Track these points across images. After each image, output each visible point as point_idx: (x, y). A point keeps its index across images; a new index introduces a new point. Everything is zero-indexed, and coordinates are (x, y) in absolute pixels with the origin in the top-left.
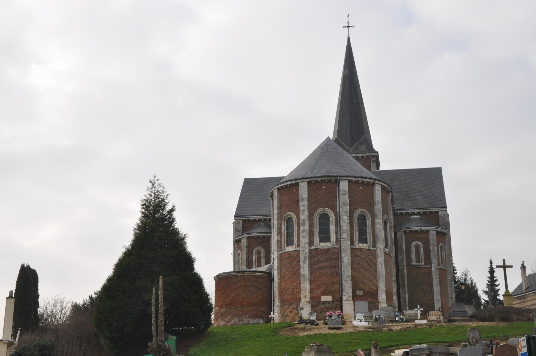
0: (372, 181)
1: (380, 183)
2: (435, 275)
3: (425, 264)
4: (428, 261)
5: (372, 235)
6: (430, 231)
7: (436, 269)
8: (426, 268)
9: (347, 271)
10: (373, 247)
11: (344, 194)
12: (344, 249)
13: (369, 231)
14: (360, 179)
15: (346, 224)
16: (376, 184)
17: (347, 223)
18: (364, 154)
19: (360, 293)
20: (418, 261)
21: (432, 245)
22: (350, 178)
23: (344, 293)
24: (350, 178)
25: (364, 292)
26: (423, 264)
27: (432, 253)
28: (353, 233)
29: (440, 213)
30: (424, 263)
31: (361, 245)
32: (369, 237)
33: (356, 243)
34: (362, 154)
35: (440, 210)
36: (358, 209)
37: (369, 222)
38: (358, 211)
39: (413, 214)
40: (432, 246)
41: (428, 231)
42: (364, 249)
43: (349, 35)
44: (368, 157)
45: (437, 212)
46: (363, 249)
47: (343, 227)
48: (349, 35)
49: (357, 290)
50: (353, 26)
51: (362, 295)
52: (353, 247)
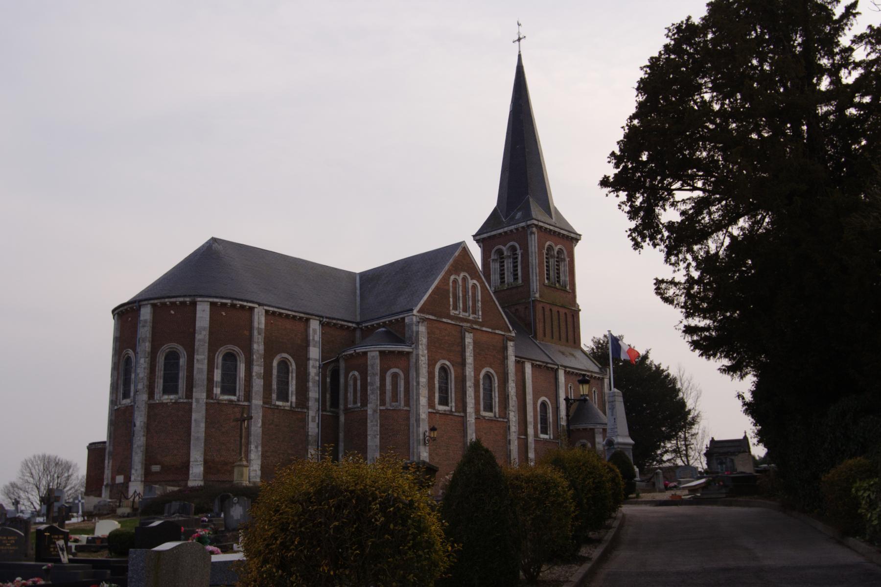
0: (188, 299)
1: (206, 299)
2: (372, 421)
3: (361, 405)
4: (365, 402)
5: (186, 381)
6: (369, 354)
7: (375, 411)
8: (362, 411)
9: (139, 438)
10: (187, 397)
11: (144, 326)
12: (137, 407)
13: (182, 374)
14: (166, 300)
15: (143, 369)
16: (198, 303)
17: (144, 368)
18: (517, 225)
19: (156, 468)
20: (355, 402)
21: (370, 375)
22: (152, 302)
23: (133, 471)
24: (152, 302)
25: (162, 467)
26: (359, 405)
27: (369, 388)
28: (155, 381)
29: (407, 320)
30: (361, 403)
31: (166, 397)
32: (182, 384)
33: (157, 396)
34: (515, 226)
35: (406, 315)
36: (164, 345)
37: (183, 361)
38: (166, 348)
39: (379, 326)
40: (371, 376)
41: (365, 353)
42: (169, 403)
43: (520, 52)
44: (523, 227)
45: (403, 319)
46: (167, 403)
47: (138, 375)
48: (520, 52)
49: (152, 465)
50: (525, 37)
51: (159, 470)
52: (151, 402)
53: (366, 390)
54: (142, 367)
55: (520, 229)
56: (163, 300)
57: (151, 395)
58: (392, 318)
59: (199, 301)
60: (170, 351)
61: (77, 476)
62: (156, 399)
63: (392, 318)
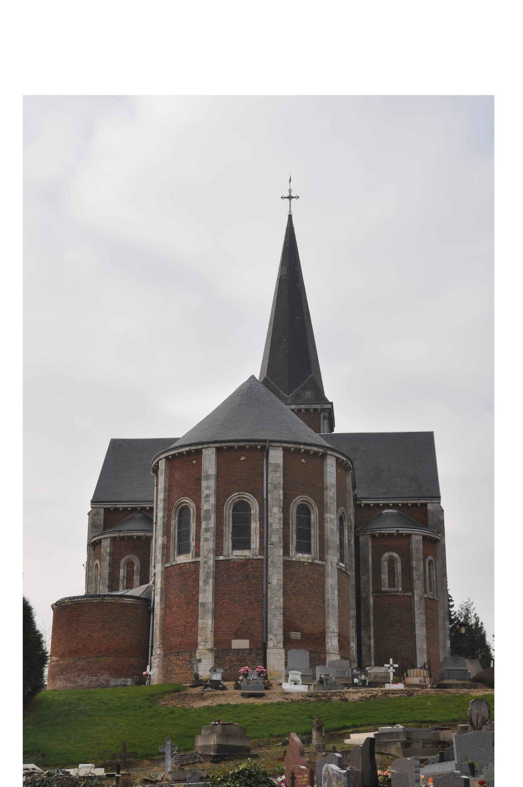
0: (321, 450)
1: (334, 454)
2: (419, 609)
3: (403, 590)
4: (409, 586)
5: (319, 540)
6: (413, 536)
7: (421, 598)
8: (404, 596)
9: (277, 598)
10: (320, 559)
11: (275, 471)
12: (272, 562)
13: (314, 532)
14: (302, 447)
15: (277, 519)
16: (328, 456)
17: (279, 519)
18: (310, 406)
19: (296, 635)
20: (392, 584)
22: (286, 445)
23: (270, 636)
24: (286, 445)
25: (303, 635)
26: (400, 589)
27: (415, 573)
28: (289, 536)
29: (429, 507)
30: (402, 587)
31: (300, 555)
32: (315, 543)
33: (292, 552)
34: (306, 406)
35: (430, 501)
36: (297, 496)
37: (314, 518)
38: (298, 500)
39: (386, 506)
40: (416, 561)
41: (409, 536)
42: (306, 562)
43: (290, 211)
44: (316, 410)
45: (425, 505)
46: (304, 562)
47: (272, 524)
48: (290, 211)
49: (292, 631)
50: (298, 197)
51: (299, 639)
52: (287, 558)
53: (359, 572)
54: (276, 517)
55: (311, 411)
56: (298, 446)
57: (286, 551)
58: (409, 502)
59: (329, 455)
60: (302, 504)
61: (353, 642)
62: (291, 556)
63: (409, 502)
